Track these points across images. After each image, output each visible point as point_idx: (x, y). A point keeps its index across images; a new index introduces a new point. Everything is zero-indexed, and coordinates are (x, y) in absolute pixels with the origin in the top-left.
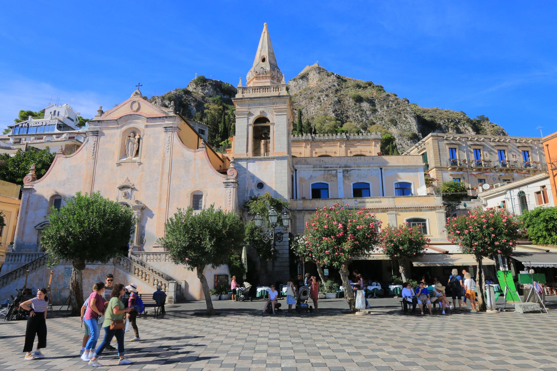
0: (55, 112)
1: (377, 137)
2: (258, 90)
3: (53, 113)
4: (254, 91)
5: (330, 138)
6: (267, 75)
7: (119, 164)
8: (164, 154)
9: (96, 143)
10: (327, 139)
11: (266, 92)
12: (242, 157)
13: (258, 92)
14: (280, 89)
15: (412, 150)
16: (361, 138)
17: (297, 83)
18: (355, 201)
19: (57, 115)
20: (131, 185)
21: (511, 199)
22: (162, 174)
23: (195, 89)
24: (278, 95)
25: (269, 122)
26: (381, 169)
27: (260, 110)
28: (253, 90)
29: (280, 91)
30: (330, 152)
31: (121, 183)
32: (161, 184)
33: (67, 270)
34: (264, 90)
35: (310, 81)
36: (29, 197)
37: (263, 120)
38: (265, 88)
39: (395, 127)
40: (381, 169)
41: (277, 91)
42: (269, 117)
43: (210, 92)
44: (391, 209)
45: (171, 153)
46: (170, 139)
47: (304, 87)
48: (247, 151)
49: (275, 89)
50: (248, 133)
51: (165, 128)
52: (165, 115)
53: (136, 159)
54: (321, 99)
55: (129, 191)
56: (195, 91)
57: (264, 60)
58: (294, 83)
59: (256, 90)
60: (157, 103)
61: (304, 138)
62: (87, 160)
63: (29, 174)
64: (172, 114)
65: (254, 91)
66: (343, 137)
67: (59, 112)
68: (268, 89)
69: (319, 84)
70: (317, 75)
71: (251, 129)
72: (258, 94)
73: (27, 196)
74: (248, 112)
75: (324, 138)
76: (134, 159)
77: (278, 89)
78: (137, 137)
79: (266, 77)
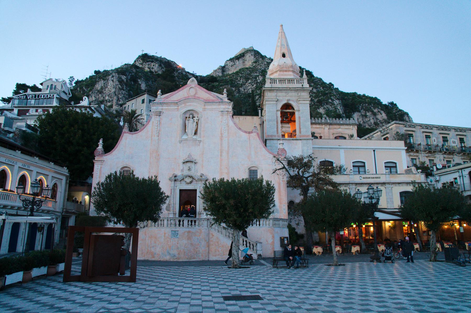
0: (52, 85)
3: (50, 87)
4: (280, 82)
7: (180, 142)
8: (221, 134)
9: (159, 122)
11: (291, 83)
12: (275, 138)
15: (374, 134)
16: (341, 122)
17: (234, 63)
19: (53, 89)
20: (193, 160)
21: (462, 176)
22: (221, 152)
23: (142, 64)
25: (294, 109)
26: (374, 151)
28: (279, 81)
29: (302, 84)
31: (184, 157)
32: (221, 160)
33: (173, 232)
35: (246, 63)
36: (101, 168)
37: (287, 106)
38: (290, 81)
39: (322, 108)
40: (374, 151)
41: (300, 83)
42: (294, 104)
43: (156, 68)
44: (389, 183)
45: (228, 133)
46: (226, 121)
47: (240, 67)
48: (278, 133)
49: (298, 82)
50: (277, 117)
51: (223, 111)
52: (220, 101)
53: (195, 137)
54: (258, 79)
55: (192, 165)
56: (141, 66)
57: (284, 56)
58: (231, 63)
59: (282, 82)
60: (114, 77)
62: (152, 136)
63: (98, 148)
64: (226, 100)
65: (280, 82)
67: (55, 86)
69: (254, 65)
70: (253, 57)
72: (284, 85)
73: (99, 167)
74: (277, 100)
76: (194, 137)
78: (195, 119)
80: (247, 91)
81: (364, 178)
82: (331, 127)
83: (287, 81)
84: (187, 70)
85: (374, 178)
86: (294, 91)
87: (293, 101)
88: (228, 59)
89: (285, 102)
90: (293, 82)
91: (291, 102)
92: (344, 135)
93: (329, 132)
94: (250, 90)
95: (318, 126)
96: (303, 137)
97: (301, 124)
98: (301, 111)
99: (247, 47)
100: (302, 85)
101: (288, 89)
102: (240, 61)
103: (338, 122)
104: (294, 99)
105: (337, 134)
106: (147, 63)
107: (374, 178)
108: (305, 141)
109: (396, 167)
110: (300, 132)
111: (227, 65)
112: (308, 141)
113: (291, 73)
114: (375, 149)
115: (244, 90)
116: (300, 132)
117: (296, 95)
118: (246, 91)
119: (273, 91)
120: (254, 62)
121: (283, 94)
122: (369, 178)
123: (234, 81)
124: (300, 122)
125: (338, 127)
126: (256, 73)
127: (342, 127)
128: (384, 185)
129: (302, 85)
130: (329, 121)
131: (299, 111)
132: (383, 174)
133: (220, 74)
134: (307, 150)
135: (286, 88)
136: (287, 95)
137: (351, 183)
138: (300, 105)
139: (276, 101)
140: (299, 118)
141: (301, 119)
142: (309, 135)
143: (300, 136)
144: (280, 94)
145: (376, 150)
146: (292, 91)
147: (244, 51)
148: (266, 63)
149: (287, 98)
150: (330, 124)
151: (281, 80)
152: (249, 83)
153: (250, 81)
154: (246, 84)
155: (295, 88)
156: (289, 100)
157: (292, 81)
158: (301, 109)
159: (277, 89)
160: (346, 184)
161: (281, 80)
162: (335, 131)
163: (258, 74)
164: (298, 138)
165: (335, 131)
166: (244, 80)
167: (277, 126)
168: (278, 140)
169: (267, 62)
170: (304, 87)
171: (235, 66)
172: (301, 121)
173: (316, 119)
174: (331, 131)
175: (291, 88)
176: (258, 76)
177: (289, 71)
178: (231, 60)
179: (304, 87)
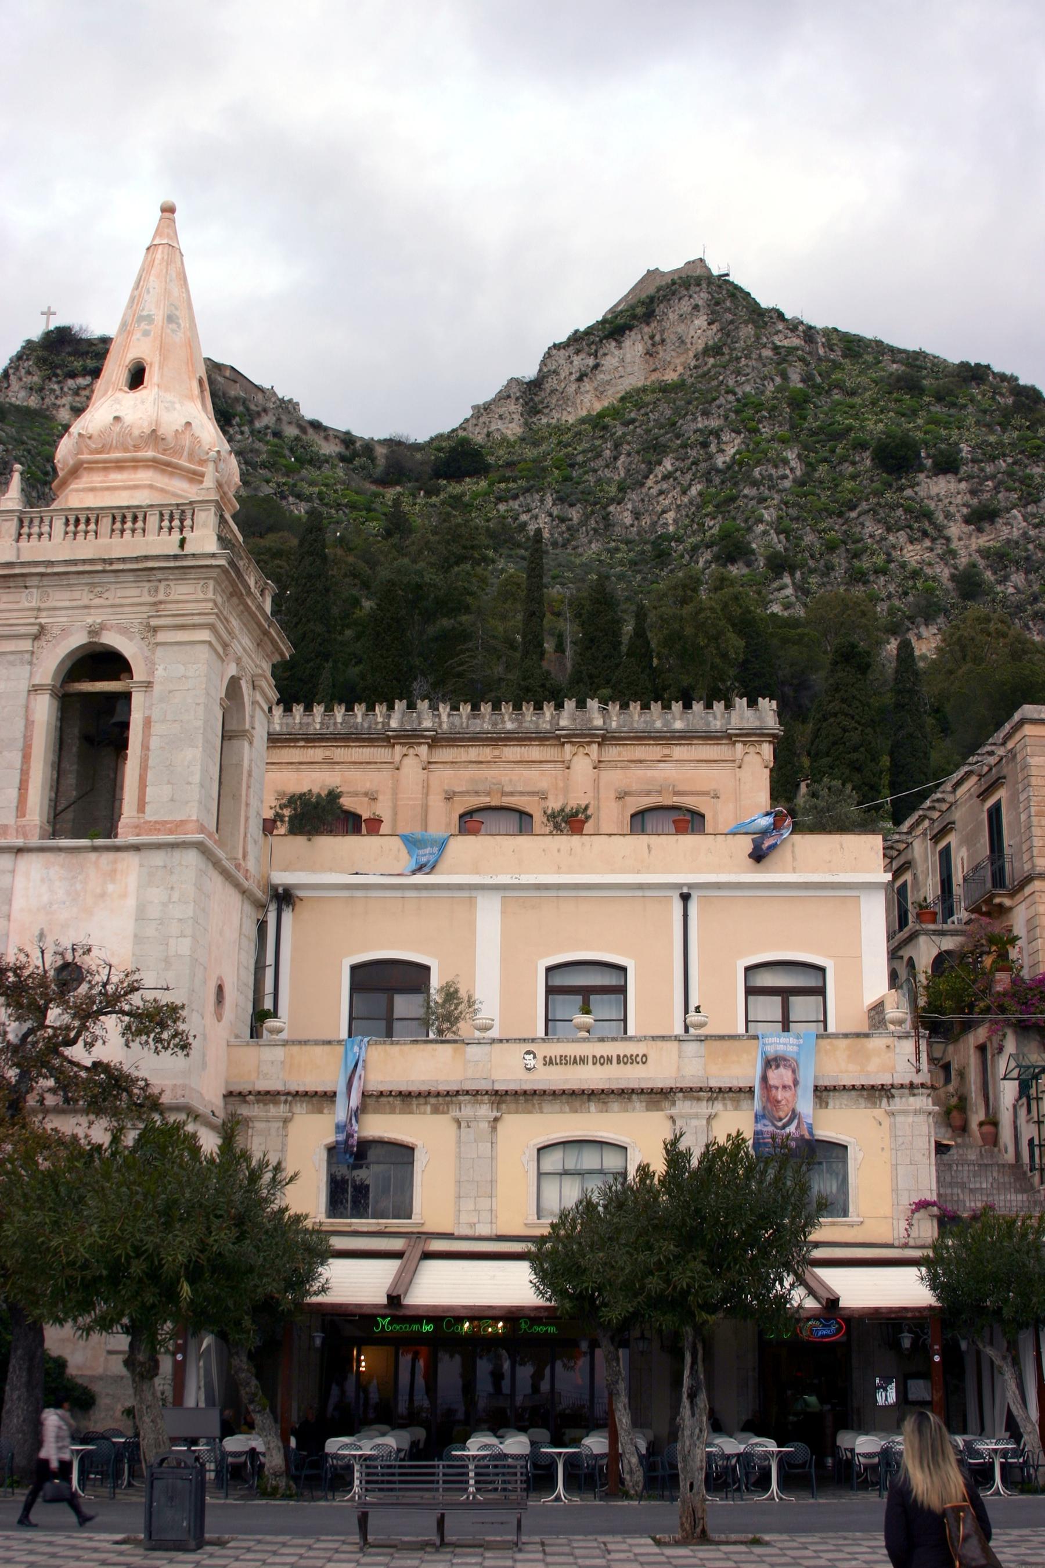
1: (757, 724)
2: (92, 526)
4: (71, 528)
5: (527, 725)
6: (140, 454)
10: (509, 726)
11: (128, 534)
13: (91, 536)
14: (188, 523)
16: (678, 725)
17: (591, 362)
18: (528, 1053)
24: (176, 551)
26: (685, 898)
27: (90, 620)
28: (67, 523)
30: (522, 793)
34: (118, 525)
35: (665, 354)
40: (685, 898)
44: (690, 1093)
50: (29, 724)
57: (137, 378)
58: (577, 360)
59: (82, 527)
61: (394, 724)
66: (590, 720)
68: (135, 519)
70: (701, 321)
71: (44, 708)
74: (35, 630)
75: (495, 724)
77: (182, 521)
79: (135, 460)
80: (654, 524)
81: (549, 1062)
82: (612, 752)
83: (106, 523)
84: (308, 412)
85: (609, 1060)
86: (130, 577)
87: (124, 631)
88: (563, 338)
89: (78, 639)
90: (140, 524)
91: (112, 639)
92: (689, 801)
93: (596, 781)
94: (670, 516)
95: (535, 752)
96: (149, 832)
97: (151, 762)
98: (157, 688)
99: (671, 262)
100: (182, 543)
101: (99, 568)
102: (627, 343)
103: (658, 724)
104: (134, 619)
105: (648, 793)
106: (70, 382)
107: (609, 1060)
108: (158, 858)
109: (820, 991)
110: (141, 807)
111: (555, 372)
112: (177, 854)
113: (145, 476)
114: (690, 886)
115: (637, 515)
116: (141, 807)
117: (147, 598)
118: (646, 521)
119: (55, 580)
120: (707, 351)
121: (83, 596)
122: (583, 1060)
123: (582, 465)
124: (145, 747)
125: (654, 752)
126: (706, 414)
127: (679, 752)
128: (667, 1104)
129: (182, 543)
130: (598, 722)
131: (148, 685)
132: (663, 1038)
133: (513, 429)
134: (164, 905)
135: (84, 562)
136: (97, 601)
137: (467, 1093)
138: (160, 652)
139: (36, 637)
140: (148, 722)
141: (157, 729)
142: (182, 822)
143: (138, 829)
144: (60, 598)
145: (695, 895)
146: (122, 577)
147: (651, 290)
148: (767, 353)
149: (93, 618)
150: (606, 739)
151: (77, 521)
152: (666, 477)
153: (668, 464)
154: (649, 483)
155: (137, 559)
156: (103, 627)
157: (135, 519)
158: (160, 672)
159: (41, 569)
160: (438, 1094)
161: (77, 521)
162: (635, 779)
163: (714, 423)
164: (119, 841)
165: (635, 779)
166: (637, 458)
167: (25, 773)
168: (19, 850)
169: (776, 349)
170: (189, 549)
171: (601, 377)
172: (154, 743)
173: (528, 709)
174: (614, 778)
175: (111, 561)
176: (716, 433)
177: (136, 464)
178: (577, 340)
179: (189, 549)
